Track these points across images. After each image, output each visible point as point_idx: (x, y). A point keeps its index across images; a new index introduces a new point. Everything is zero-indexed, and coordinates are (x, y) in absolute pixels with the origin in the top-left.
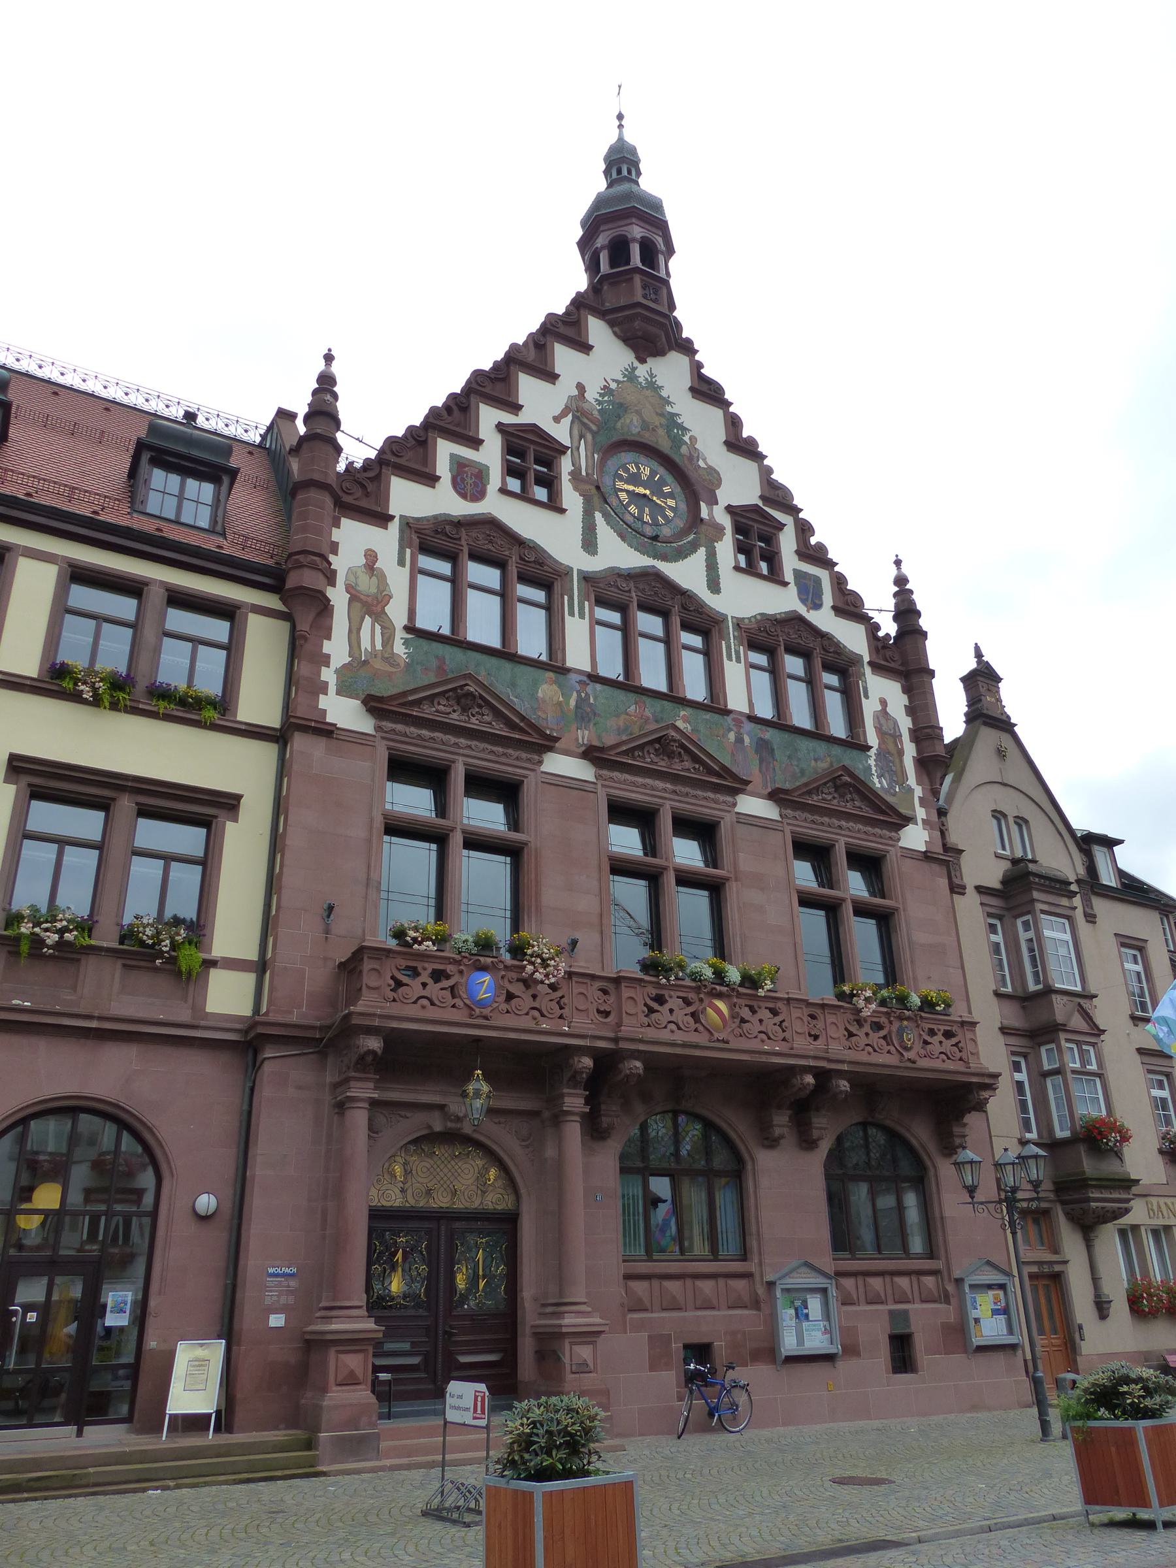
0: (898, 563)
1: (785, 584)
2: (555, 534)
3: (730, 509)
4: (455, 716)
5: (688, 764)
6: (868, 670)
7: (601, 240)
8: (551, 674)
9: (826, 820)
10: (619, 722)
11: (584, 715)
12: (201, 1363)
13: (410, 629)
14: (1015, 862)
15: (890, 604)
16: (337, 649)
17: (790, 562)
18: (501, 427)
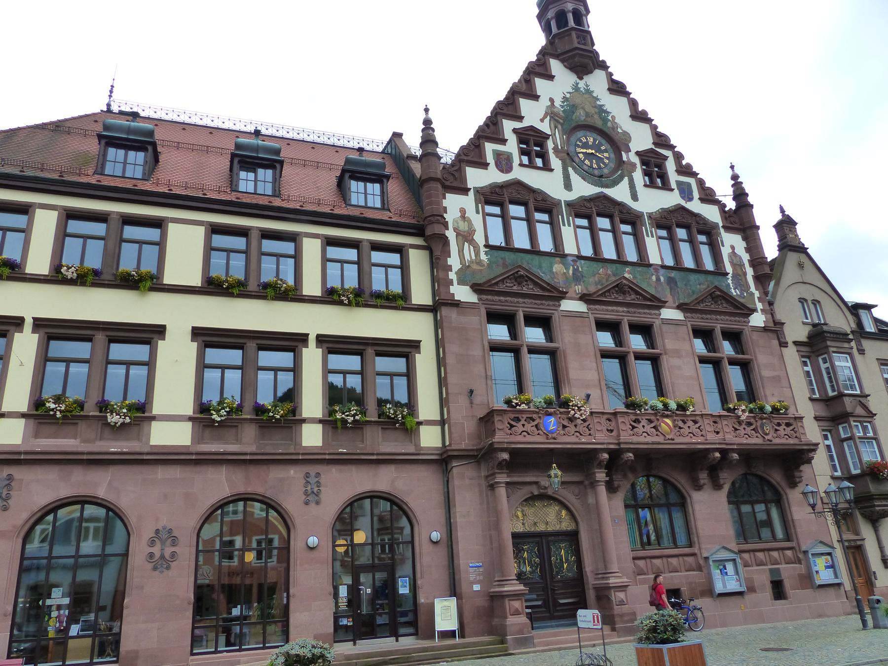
0: (732, 167)
1: (672, 190)
2: (549, 183)
3: (638, 153)
4: (515, 288)
5: (633, 297)
6: (722, 230)
7: (551, 14)
8: (558, 259)
9: (709, 316)
10: (596, 279)
11: (578, 277)
12: (447, 608)
13: (487, 246)
14: (814, 325)
15: (730, 191)
16: (454, 261)
17: (673, 177)
18: (515, 131)
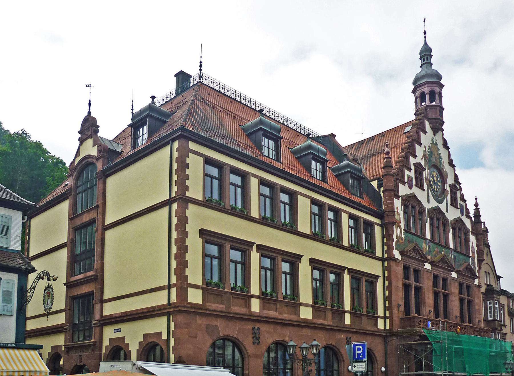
0: (476, 199)
11: (429, 251)
14: (488, 285)
17: (459, 202)
